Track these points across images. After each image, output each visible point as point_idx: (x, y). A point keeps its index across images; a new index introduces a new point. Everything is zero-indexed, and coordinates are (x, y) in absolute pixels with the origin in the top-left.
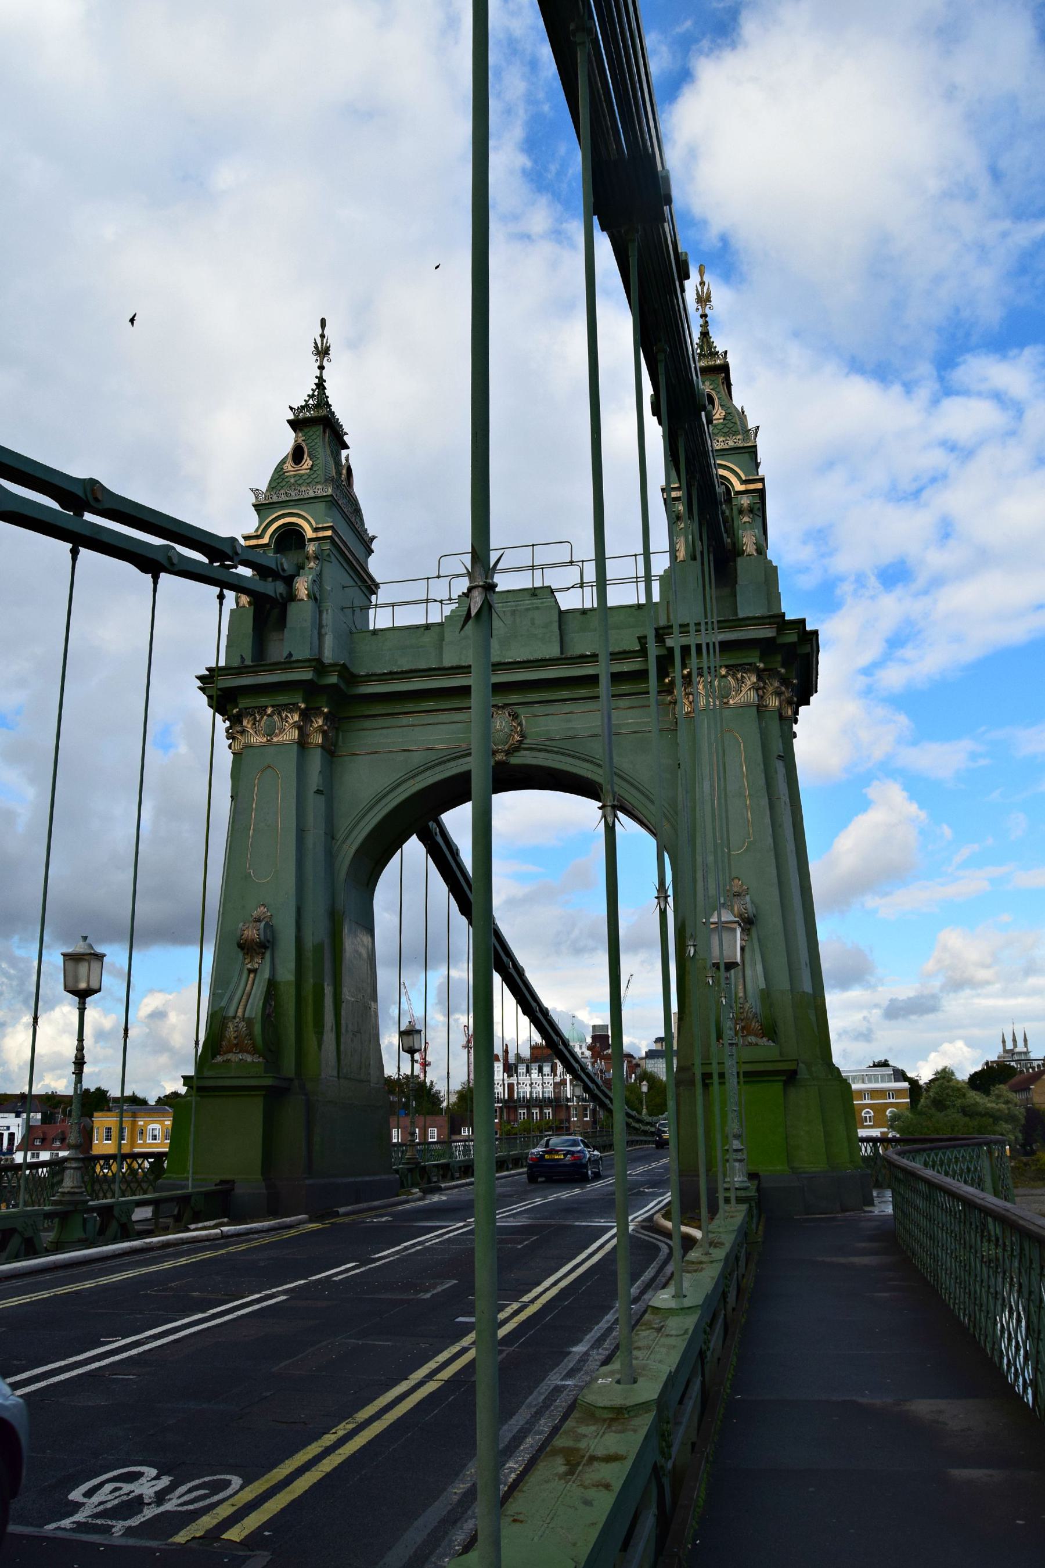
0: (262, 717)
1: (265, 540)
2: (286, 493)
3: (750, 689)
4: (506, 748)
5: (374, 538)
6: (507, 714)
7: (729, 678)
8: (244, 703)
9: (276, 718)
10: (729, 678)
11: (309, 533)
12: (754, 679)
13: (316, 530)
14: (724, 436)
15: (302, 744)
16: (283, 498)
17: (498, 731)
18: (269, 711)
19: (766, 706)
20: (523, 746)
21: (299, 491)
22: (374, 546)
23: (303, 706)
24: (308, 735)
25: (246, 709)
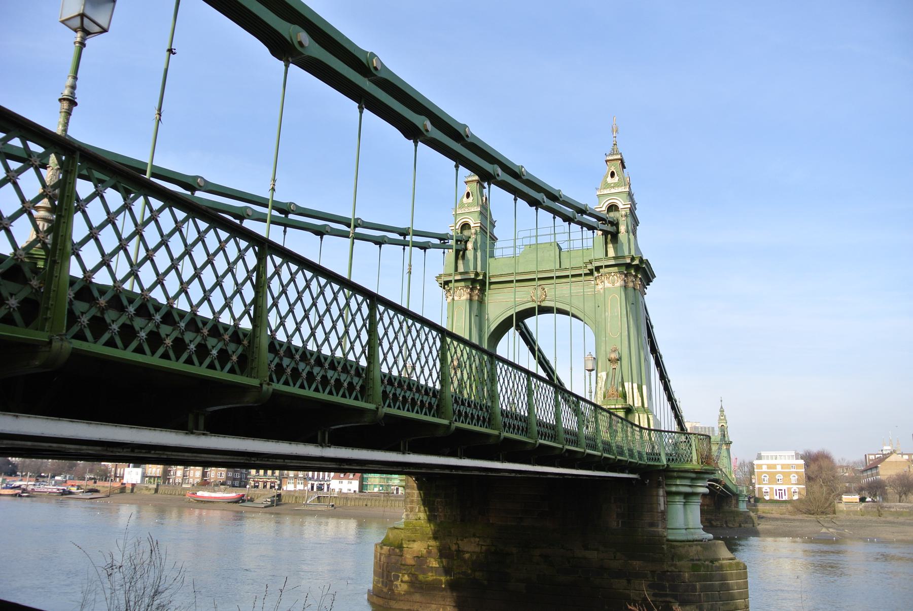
5: (496, 221)
7: (615, 276)
10: (615, 276)
11: (472, 225)
12: (623, 277)
15: (471, 300)
18: (460, 288)
22: (495, 225)
23: (471, 287)
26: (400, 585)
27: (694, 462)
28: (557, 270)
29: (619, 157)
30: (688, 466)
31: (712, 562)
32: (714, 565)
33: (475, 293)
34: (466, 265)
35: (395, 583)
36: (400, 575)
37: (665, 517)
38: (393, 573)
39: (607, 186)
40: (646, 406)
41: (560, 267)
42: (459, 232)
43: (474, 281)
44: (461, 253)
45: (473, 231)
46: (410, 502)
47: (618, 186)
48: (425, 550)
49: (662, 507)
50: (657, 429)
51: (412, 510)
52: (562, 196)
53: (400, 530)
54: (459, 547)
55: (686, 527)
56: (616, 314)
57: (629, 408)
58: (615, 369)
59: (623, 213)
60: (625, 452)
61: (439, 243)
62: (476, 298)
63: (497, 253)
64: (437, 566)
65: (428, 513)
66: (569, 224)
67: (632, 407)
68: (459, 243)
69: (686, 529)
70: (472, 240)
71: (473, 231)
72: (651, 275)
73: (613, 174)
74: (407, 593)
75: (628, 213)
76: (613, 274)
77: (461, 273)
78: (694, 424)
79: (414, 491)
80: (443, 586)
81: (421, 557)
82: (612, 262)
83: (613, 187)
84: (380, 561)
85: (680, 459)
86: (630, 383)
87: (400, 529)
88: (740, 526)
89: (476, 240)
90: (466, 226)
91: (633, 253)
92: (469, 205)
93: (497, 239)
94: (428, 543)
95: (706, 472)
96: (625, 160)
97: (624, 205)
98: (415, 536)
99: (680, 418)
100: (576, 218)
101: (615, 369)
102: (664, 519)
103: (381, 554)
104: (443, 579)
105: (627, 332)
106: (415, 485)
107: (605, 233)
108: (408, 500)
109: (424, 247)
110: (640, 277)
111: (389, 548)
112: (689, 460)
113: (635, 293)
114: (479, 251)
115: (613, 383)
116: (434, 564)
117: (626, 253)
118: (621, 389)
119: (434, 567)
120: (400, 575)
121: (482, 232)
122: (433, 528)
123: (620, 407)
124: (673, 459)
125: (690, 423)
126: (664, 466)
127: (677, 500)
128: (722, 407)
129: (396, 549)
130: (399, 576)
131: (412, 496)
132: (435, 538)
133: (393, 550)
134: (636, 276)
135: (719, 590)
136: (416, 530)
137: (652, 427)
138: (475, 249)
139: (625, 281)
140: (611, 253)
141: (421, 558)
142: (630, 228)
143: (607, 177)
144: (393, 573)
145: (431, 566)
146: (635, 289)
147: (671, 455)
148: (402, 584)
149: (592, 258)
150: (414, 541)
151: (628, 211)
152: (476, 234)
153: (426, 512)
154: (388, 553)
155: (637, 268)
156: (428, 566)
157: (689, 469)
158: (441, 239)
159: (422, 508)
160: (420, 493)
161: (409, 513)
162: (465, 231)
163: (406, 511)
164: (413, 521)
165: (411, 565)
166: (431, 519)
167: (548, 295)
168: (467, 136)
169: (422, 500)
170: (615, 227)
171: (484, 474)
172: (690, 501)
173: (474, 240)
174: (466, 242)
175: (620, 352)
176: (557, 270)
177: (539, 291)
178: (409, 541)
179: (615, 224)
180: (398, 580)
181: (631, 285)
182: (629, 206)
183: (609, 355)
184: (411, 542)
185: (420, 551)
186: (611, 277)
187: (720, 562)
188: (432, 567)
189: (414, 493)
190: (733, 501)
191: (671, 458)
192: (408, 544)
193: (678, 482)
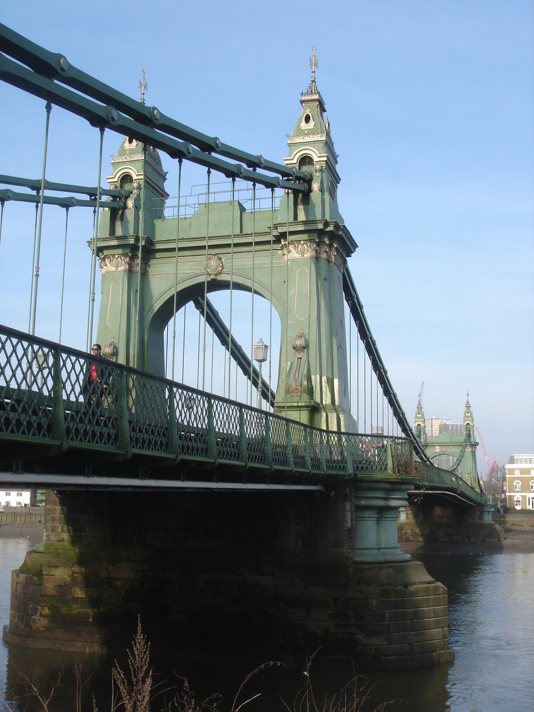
0: (114, 259)
1: (116, 180)
3: (313, 250)
4: (216, 273)
5: (167, 173)
6: (216, 258)
7: (305, 245)
8: (106, 252)
9: (119, 259)
10: (305, 245)
11: (135, 177)
12: (315, 246)
14: (312, 135)
17: (212, 266)
18: (117, 256)
19: (321, 257)
22: (167, 177)
23: (130, 255)
24: (133, 267)
25: (107, 255)
26: (39, 620)
27: (390, 471)
28: (236, 236)
29: (317, 97)
30: (379, 476)
31: (406, 586)
32: (407, 590)
33: (136, 262)
34: (125, 228)
35: (33, 617)
36: (39, 607)
37: (352, 535)
38: (30, 606)
39: (300, 132)
40: (337, 403)
41: (241, 232)
42: (118, 185)
43: (134, 248)
44: (120, 212)
45: (135, 185)
47: (313, 134)
48: (69, 578)
49: (349, 525)
50: (351, 431)
51: (53, 529)
52: (220, 146)
53: (39, 554)
55: (378, 547)
56: (305, 292)
57: (313, 406)
58: (301, 358)
59: (318, 167)
60: (290, 460)
61: (89, 199)
62: (138, 269)
63: (168, 213)
64: (84, 596)
65: (72, 533)
66: (234, 180)
67: (319, 405)
68: (118, 199)
69: (378, 549)
70: (133, 196)
71: (135, 185)
72: (352, 244)
73: (307, 119)
74: (47, 628)
75: (324, 168)
76: (302, 242)
77: (118, 238)
78: (444, 422)
79: (56, 507)
80: (91, 620)
81: (65, 586)
82: (301, 228)
83: (307, 135)
84: (16, 591)
85: (372, 466)
86: (318, 376)
87: (40, 552)
88: (484, 541)
89: (139, 196)
90: (126, 178)
91: (327, 217)
92: (132, 152)
93: (168, 195)
94: (73, 569)
95: (404, 482)
96: (325, 100)
97: (319, 157)
99: (401, 416)
100: (241, 173)
101: (301, 358)
102: (351, 538)
103: (17, 583)
104: (90, 611)
105: (316, 314)
106: (57, 499)
107: (296, 192)
108: (49, 518)
109: (66, 204)
110: (335, 246)
111: (26, 575)
112: (383, 468)
113: (329, 267)
114: (141, 210)
115: (297, 376)
116: (79, 593)
117: (319, 217)
118: (306, 383)
119: (80, 597)
120: (39, 607)
121: (147, 185)
122: (77, 551)
123: (303, 404)
124: (362, 468)
125: (440, 421)
126: (350, 475)
127: (367, 516)
128: (468, 402)
129: (34, 577)
130: (38, 609)
132: (80, 562)
133: (31, 578)
134: (330, 246)
135: (412, 618)
137: (343, 430)
138: (137, 207)
139: (316, 251)
140: (302, 217)
141: (65, 587)
142: (325, 186)
143: (301, 122)
144: (30, 606)
145: (76, 596)
146: (329, 261)
147: (360, 463)
148: (42, 619)
149: (279, 221)
150: (56, 567)
151: (324, 165)
152: (139, 188)
154: (25, 582)
155: (332, 236)
156: (73, 597)
157: (382, 479)
158: (91, 195)
159: (65, 528)
160: (63, 509)
161: (50, 533)
162: (126, 184)
163: (47, 531)
164: (55, 543)
165: (54, 596)
166: (74, 541)
167: (225, 266)
168: (63, 70)
169: (65, 517)
170: (306, 185)
171: (84, 490)
172: (384, 516)
173: (135, 196)
174: (127, 198)
175: (307, 338)
176: (236, 236)
177: (214, 262)
178: (50, 567)
179: (309, 181)
180: (37, 614)
181: (324, 256)
182: (325, 159)
183: (293, 342)
184: (52, 568)
185: (63, 579)
186: (300, 245)
187: (415, 586)
188: (77, 598)
189: (56, 510)
190: (477, 512)
191: (360, 466)
193: (370, 494)
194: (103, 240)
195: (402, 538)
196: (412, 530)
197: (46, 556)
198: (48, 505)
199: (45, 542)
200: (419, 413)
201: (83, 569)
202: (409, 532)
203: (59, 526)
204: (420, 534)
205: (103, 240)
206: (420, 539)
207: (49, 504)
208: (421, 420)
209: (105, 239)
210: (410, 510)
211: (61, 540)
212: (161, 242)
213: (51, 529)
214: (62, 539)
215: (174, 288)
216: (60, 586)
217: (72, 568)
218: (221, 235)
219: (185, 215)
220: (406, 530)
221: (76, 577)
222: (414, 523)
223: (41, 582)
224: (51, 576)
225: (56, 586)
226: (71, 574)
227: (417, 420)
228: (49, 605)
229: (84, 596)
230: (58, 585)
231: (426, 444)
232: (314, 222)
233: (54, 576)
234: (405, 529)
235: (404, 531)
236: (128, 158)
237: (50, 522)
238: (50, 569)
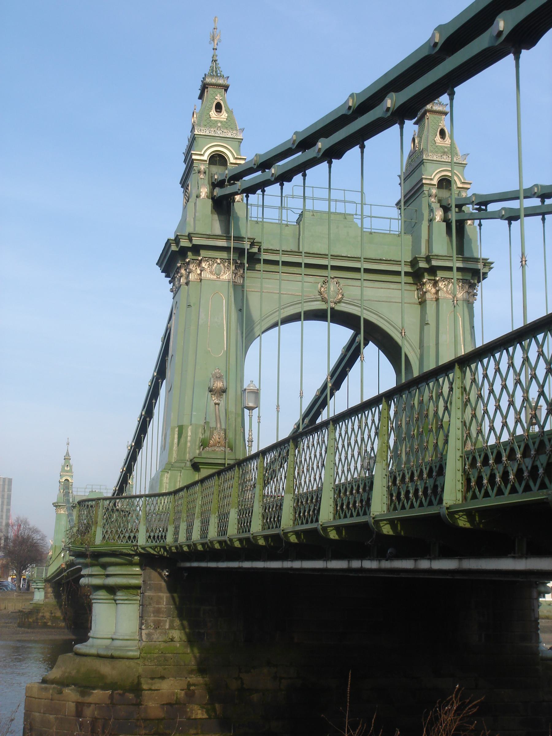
2: (215, 131)
8: (203, 253)
9: (221, 265)
13: (236, 158)
16: (212, 134)
20: (343, 301)
21: (223, 132)
46: (153, 614)
48: (183, 692)
53: (136, 661)
54: (242, 683)
64: (205, 716)
65: (187, 630)
79: (161, 594)
98: (165, 669)
106: (164, 584)
111: (110, 692)
116: (199, 714)
119: (200, 719)
131: (158, 603)
132: (202, 670)
136: (166, 660)
145: (193, 717)
150: (163, 678)
153: (184, 628)
154: (108, 702)
156: (189, 719)
159: (177, 622)
163: (147, 628)
165: (158, 719)
178: (152, 678)
185: (173, 694)
188: (195, 719)
192: (152, 684)
194: (207, 236)
195: (37, 623)
196: (51, 613)
197: (147, 664)
198: (148, 592)
199: (145, 643)
200: (67, 466)
201: (207, 679)
202: (47, 615)
203: (166, 621)
204: (62, 618)
205: (207, 236)
206: (60, 625)
207: (149, 590)
208: (70, 474)
209: (211, 237)
210: (51, 587)
211: (170, 640)
212: (270, 251)
213: (154, 625)
214: (171, 639)
215: (277, 313)
216: (170, 704)
217: (186, 678)
218: (349, 256)
219: (390, 231)
220: (43, 613)
221: (193, 690)
222: (55, 603)
223: (139, 700)
224: (156, 692)
225: (164, 704)
226: (186, 687)
227: (64, 474)
228: (152, 733)
229: (205, 716)
230: (165, 702)
231: (74, 505)
232: (475, 260)
233: (161, 691)
234: (43, 611)
235: (40, 614)
236: (219, 132)
237: (152, 615)
238: (153, 681)
